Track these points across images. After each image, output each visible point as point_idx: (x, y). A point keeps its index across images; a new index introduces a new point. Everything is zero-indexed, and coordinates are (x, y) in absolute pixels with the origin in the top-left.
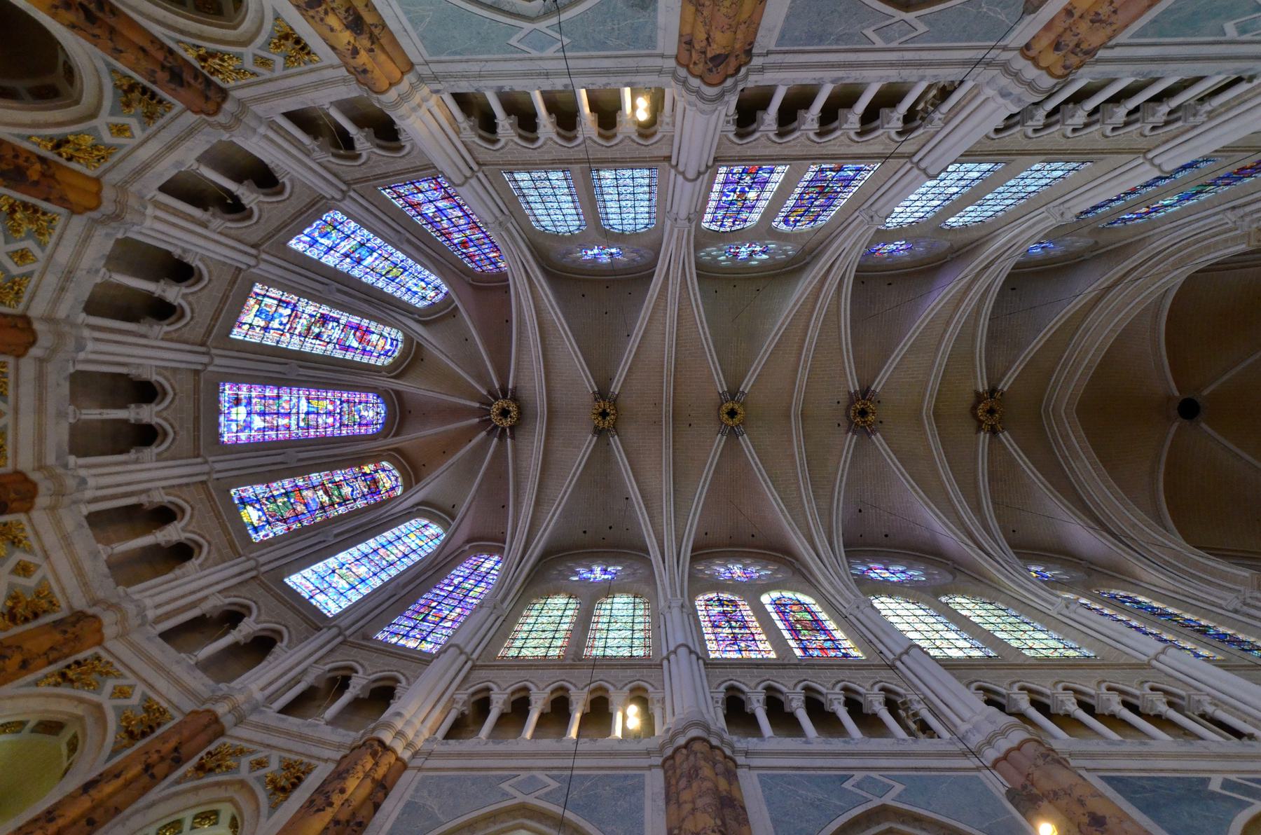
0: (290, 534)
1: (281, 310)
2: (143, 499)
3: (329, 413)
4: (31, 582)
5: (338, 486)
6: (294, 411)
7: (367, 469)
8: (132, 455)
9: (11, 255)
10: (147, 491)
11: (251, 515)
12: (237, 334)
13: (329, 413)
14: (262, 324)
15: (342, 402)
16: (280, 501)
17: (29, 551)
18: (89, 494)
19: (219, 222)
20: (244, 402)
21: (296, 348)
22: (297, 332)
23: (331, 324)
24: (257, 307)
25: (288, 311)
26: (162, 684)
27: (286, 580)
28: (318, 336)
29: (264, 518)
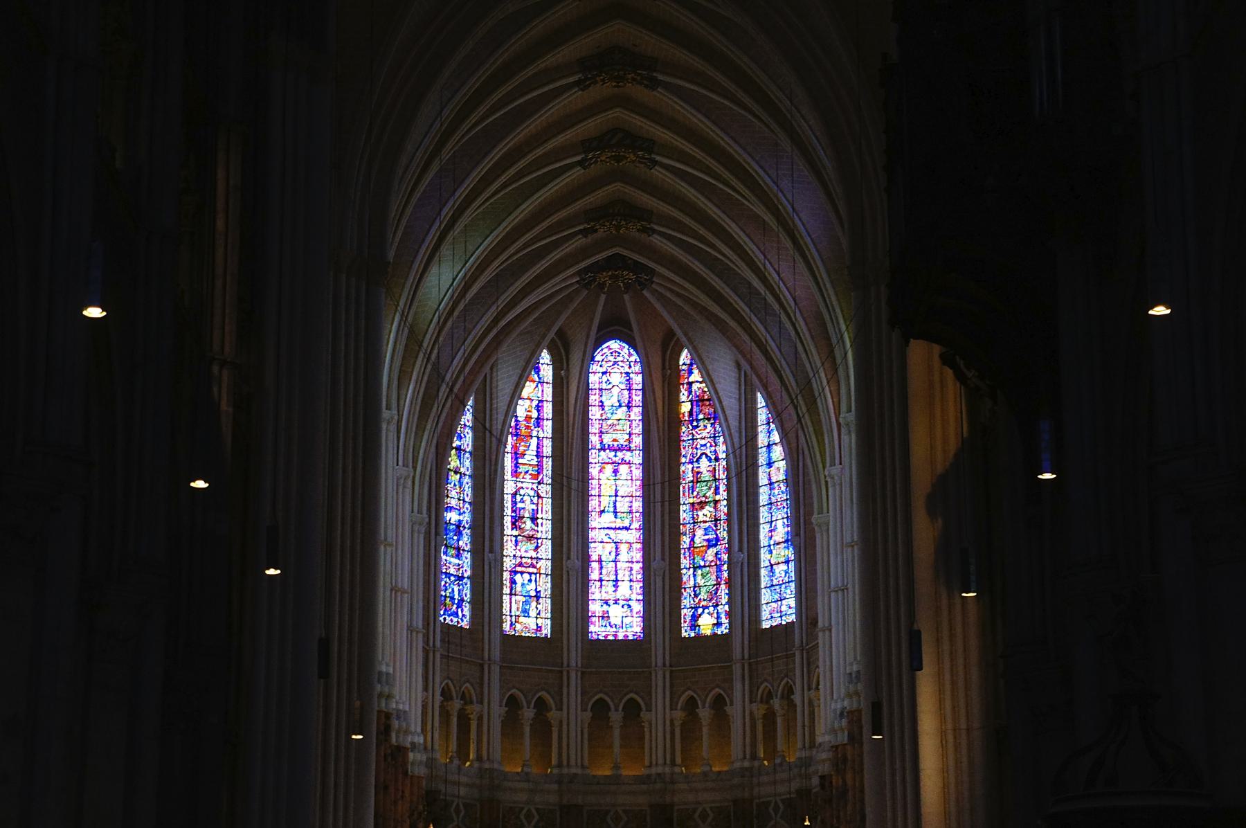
0: (729, 583)
1: (518, 588)
2: (677, 723)
3: (616, 472)
4: (712, 815)
5: (697, 479)
6: (611, 532)
7: (686, 408)
8: (646, 725)
9: (529, 823)
10: (672, 721)
11: (706, 624)
12: (547, 631)
13: (616, 472)
14: (534, 604)
15: (603, 449)
16: (700, 581)
17: (694, 811)
18: (667, 770)
19: (474, 710)
20: (605, 608)
21: (549, 563)
22: (534, 555)
23: (520, 505)
24: (522, 619)
25: (518, 578)
26: (781, 789)
27: (766, 625)
28: (534, 519)
29: (711, 609)
